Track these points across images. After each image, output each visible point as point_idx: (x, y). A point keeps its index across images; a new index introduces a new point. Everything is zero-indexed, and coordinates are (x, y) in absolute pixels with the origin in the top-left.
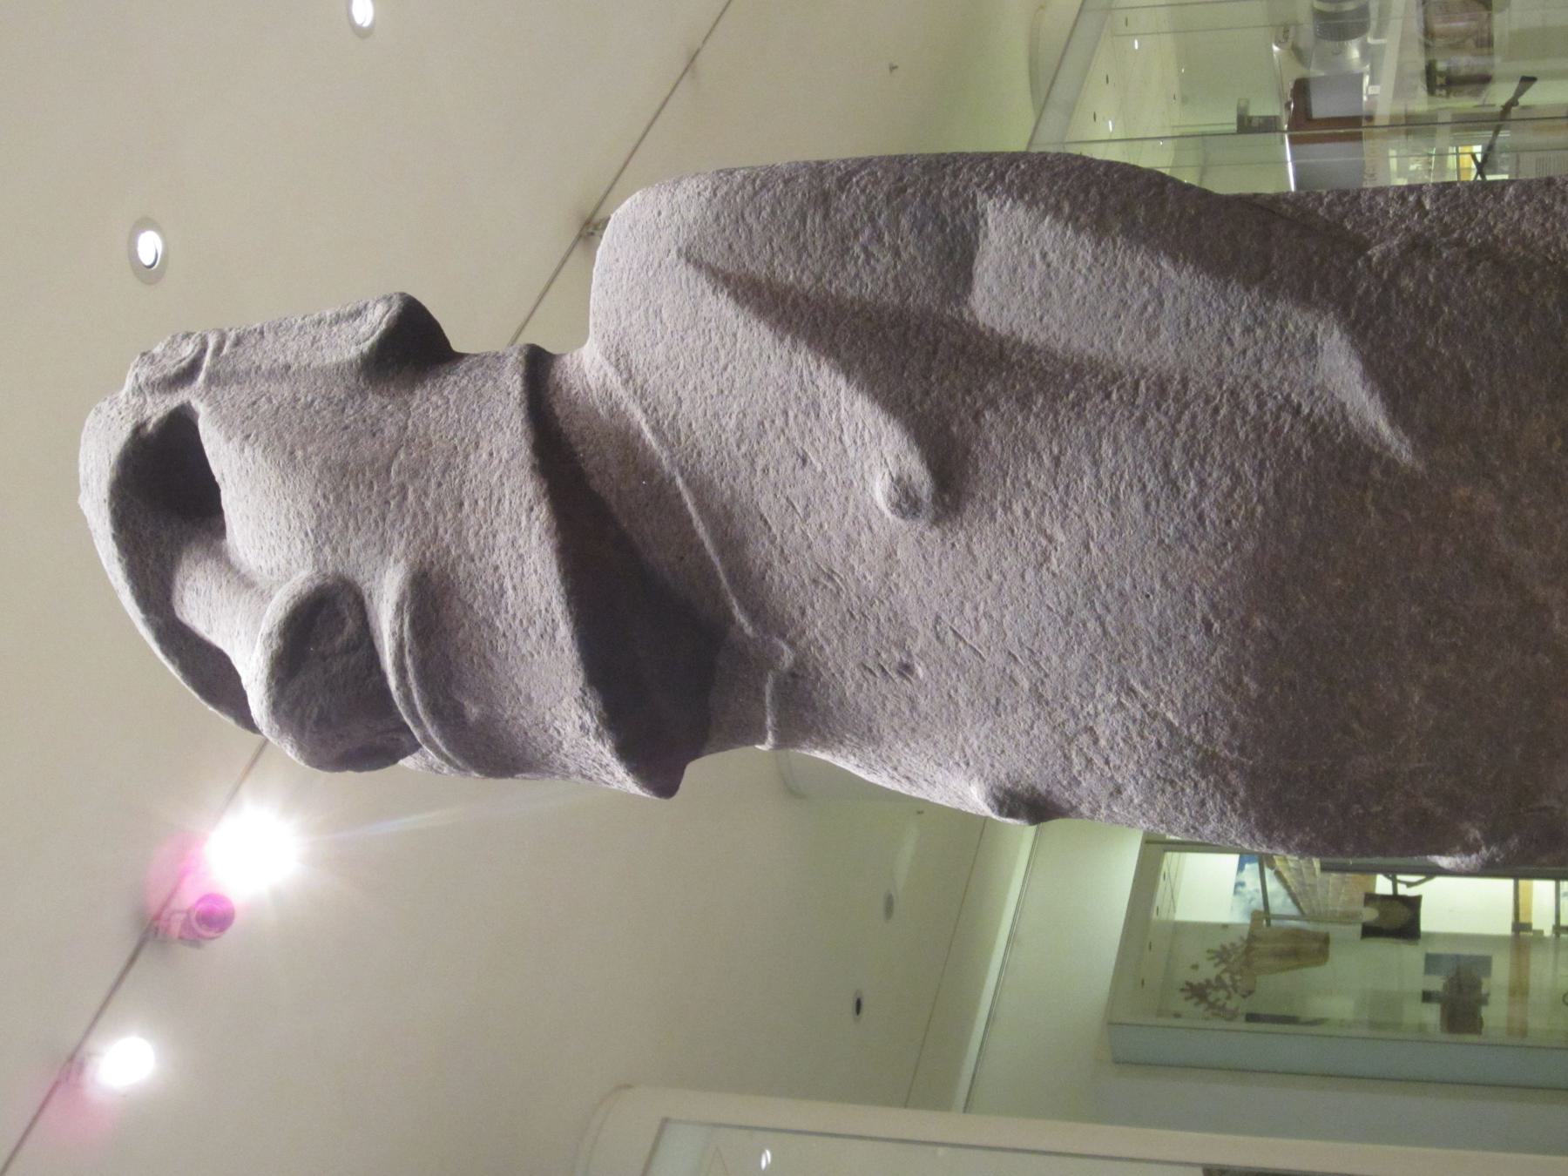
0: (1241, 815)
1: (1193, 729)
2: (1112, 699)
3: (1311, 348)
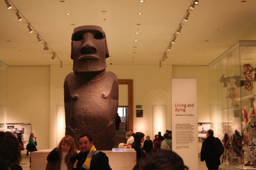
2: (90, 107)
3: (112, 121)
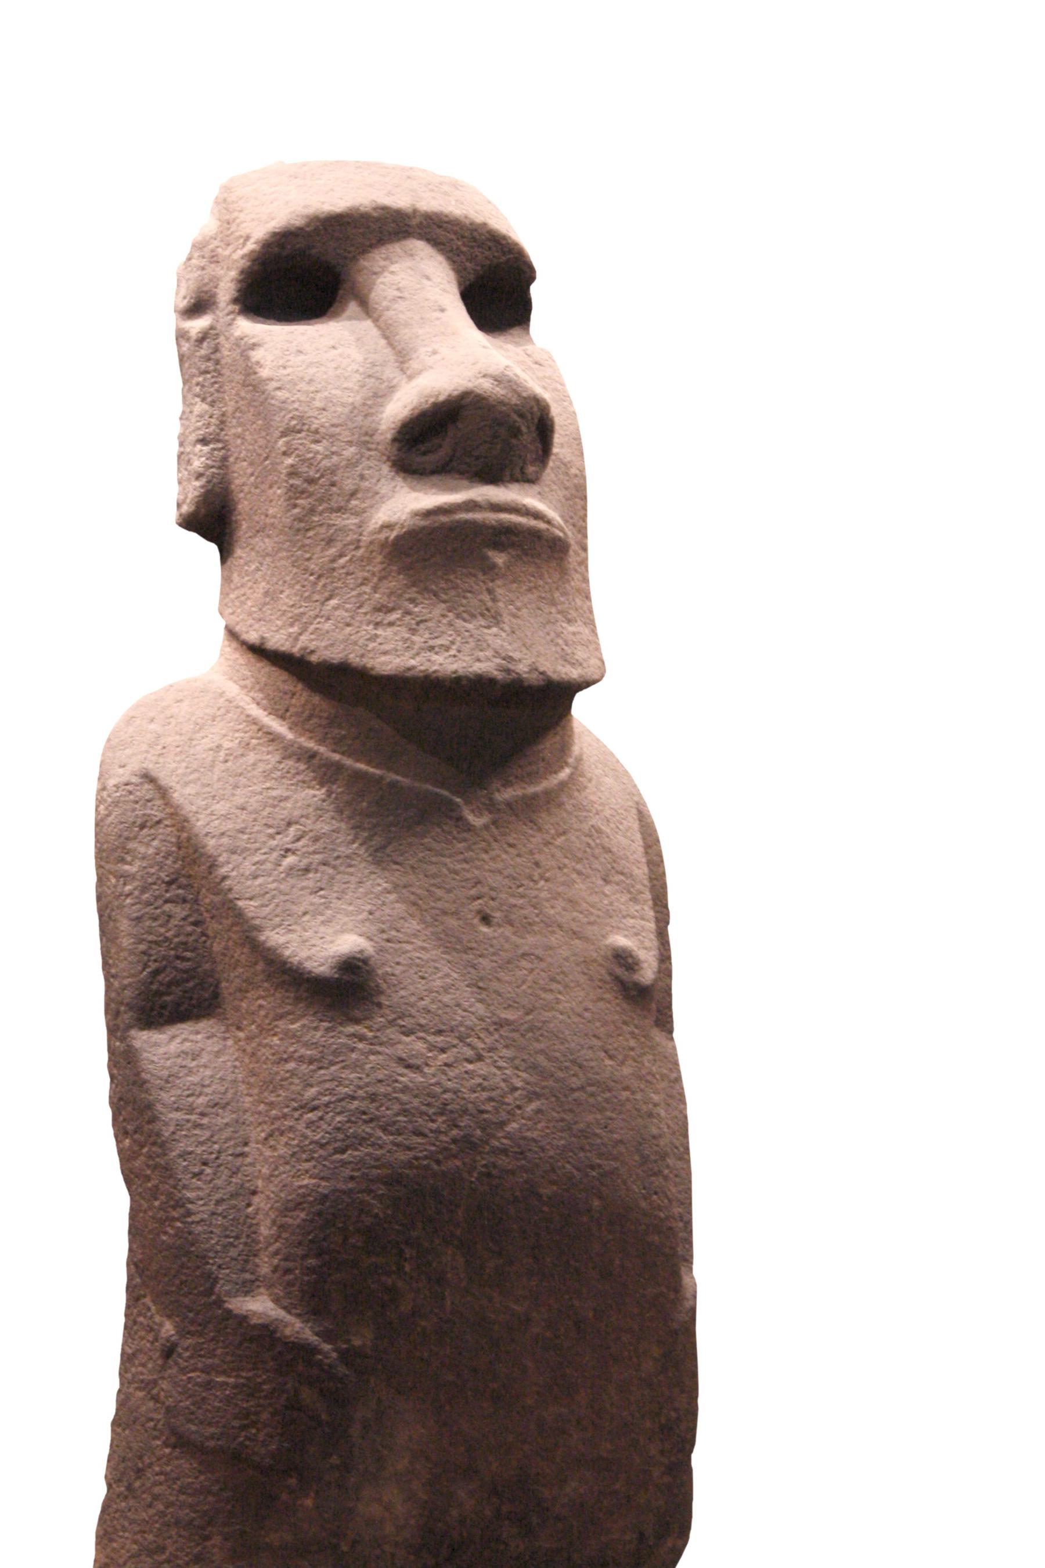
0: (410, 1162)
1: (504, 1141)
